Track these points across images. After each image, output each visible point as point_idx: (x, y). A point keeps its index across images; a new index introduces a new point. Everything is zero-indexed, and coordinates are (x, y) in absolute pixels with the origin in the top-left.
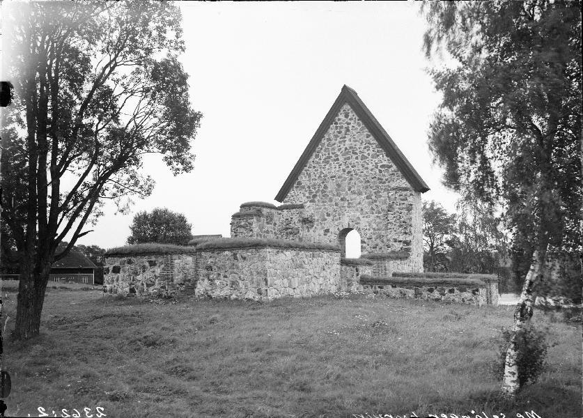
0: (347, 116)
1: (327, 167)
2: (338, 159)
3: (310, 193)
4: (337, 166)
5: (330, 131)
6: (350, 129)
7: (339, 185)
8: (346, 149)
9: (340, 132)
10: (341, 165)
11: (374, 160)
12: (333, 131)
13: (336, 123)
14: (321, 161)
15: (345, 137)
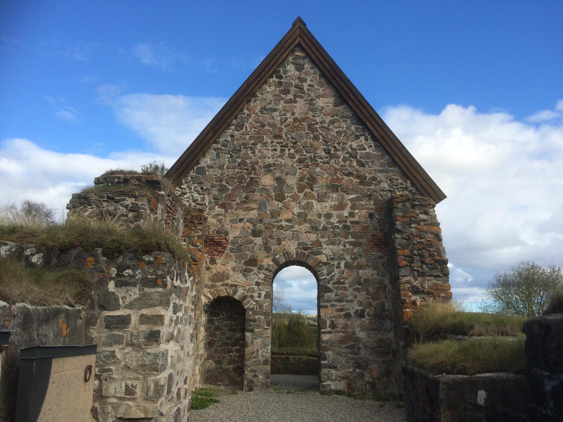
0: (299, 68)
1: (259, 146)
2: (280, 137)
3: (223, 189)
4: (279, 148)
5: (267, 88)
6: (306, 87)
7: (279, 180)
8: (295, 120)
9: (287, 92)
10: (286, 146)
11: (349, 143)
12: (273, 88)
13: (280, 77)
14: (247, 137)
15: (296, 102)
